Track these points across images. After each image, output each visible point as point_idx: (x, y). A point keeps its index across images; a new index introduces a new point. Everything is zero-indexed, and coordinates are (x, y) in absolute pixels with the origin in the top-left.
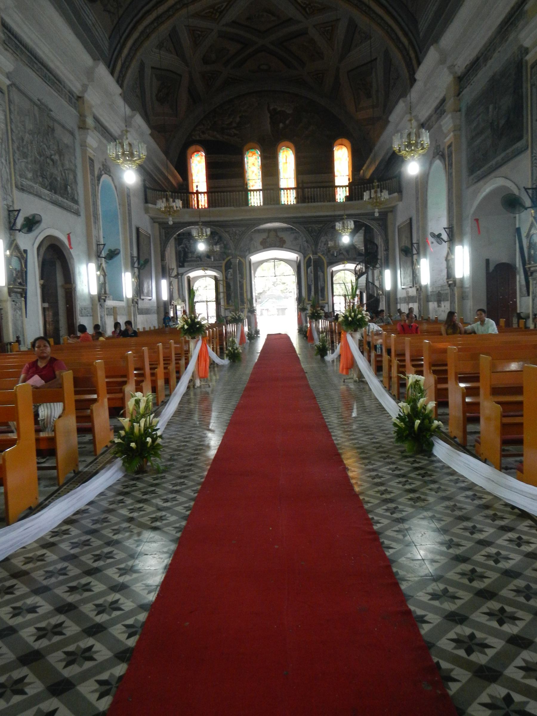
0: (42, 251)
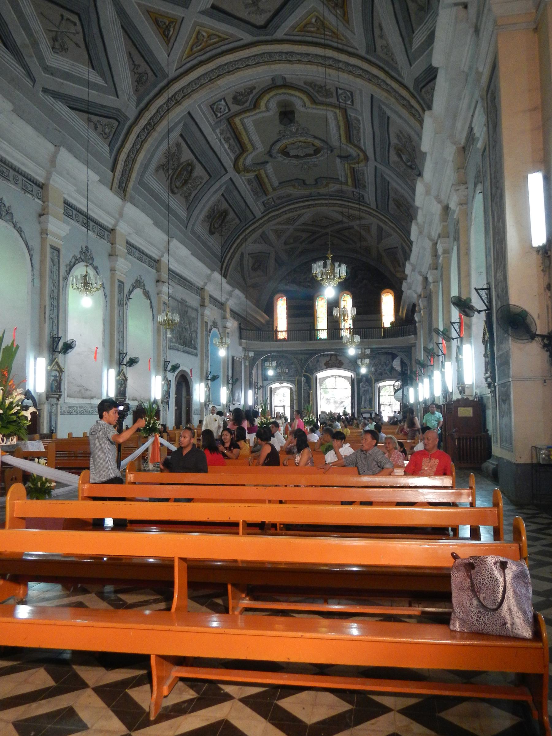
0: (177, 379)
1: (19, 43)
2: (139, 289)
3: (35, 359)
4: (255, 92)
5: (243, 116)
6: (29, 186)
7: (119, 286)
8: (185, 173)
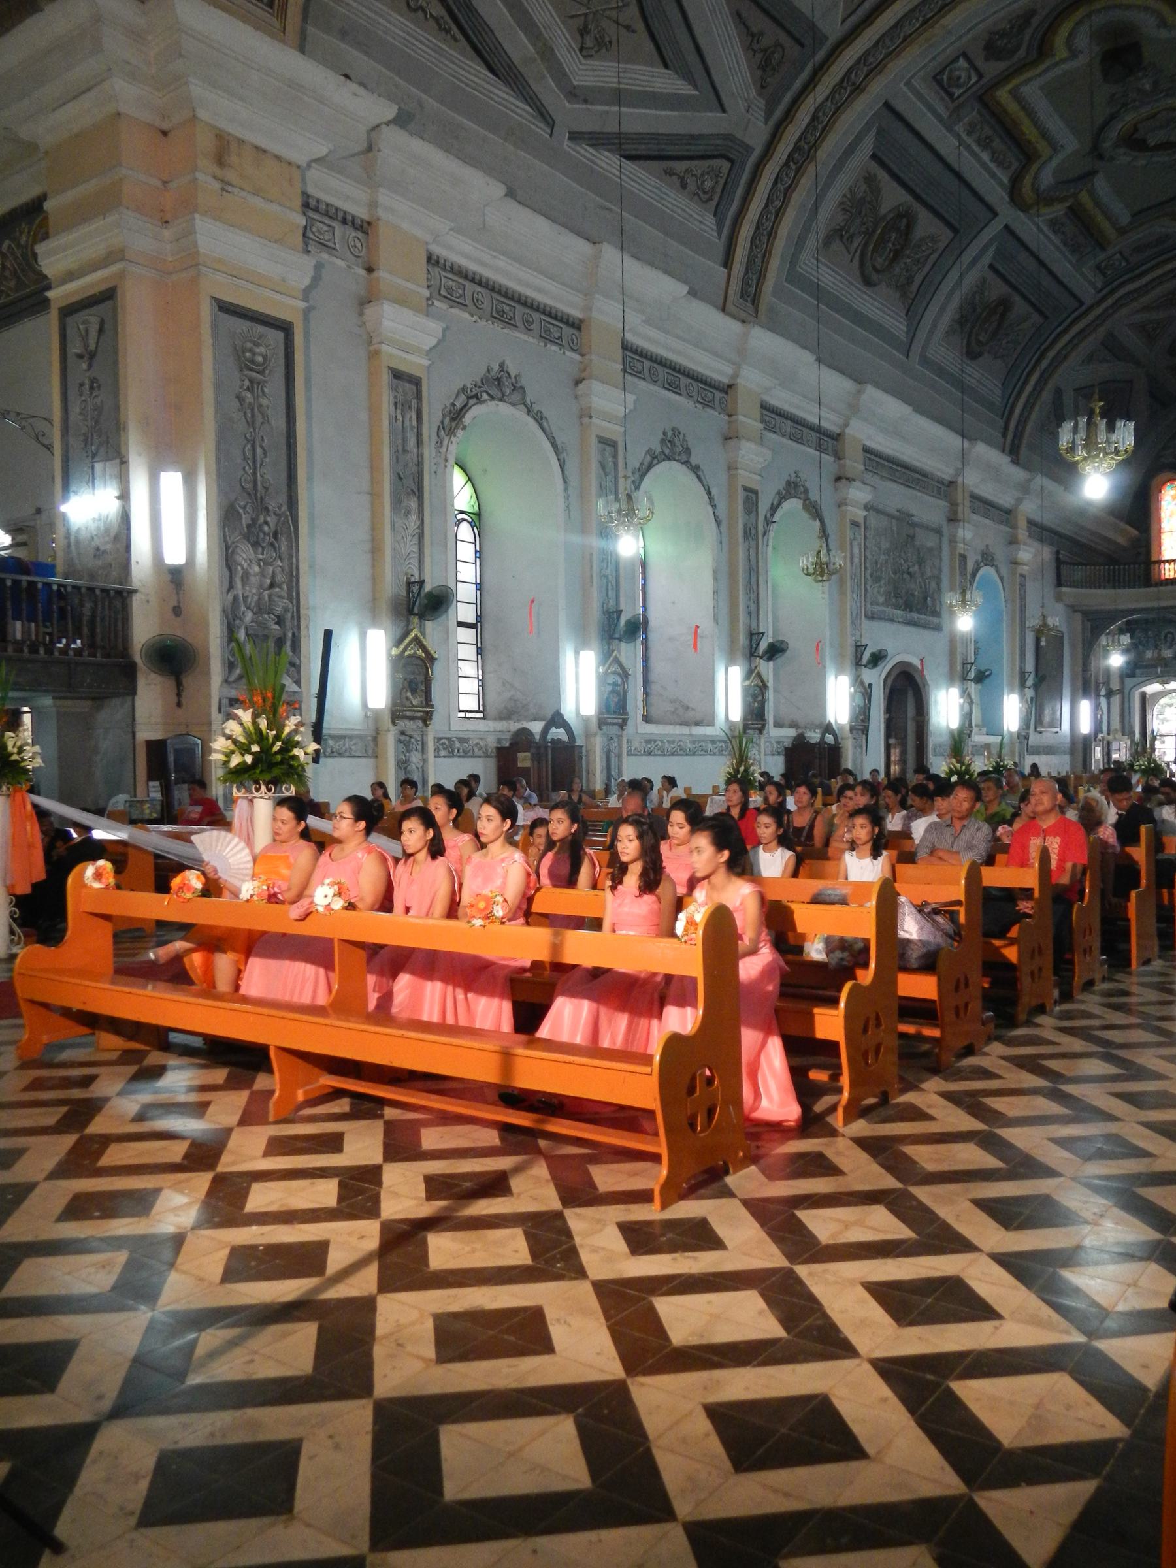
0: (889, 683)
1: (516, 57)
2: (794, 500)
3: (577, 653)
4: (1035, 21)
5: (1015, 82)
6: (553, 329)
7: (747, 500)
8: (894, 235)
